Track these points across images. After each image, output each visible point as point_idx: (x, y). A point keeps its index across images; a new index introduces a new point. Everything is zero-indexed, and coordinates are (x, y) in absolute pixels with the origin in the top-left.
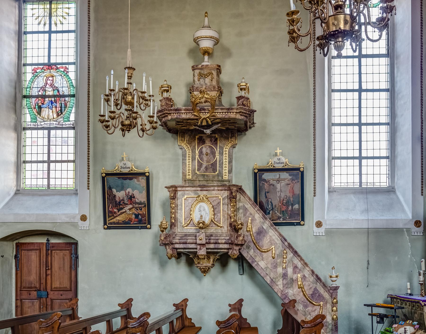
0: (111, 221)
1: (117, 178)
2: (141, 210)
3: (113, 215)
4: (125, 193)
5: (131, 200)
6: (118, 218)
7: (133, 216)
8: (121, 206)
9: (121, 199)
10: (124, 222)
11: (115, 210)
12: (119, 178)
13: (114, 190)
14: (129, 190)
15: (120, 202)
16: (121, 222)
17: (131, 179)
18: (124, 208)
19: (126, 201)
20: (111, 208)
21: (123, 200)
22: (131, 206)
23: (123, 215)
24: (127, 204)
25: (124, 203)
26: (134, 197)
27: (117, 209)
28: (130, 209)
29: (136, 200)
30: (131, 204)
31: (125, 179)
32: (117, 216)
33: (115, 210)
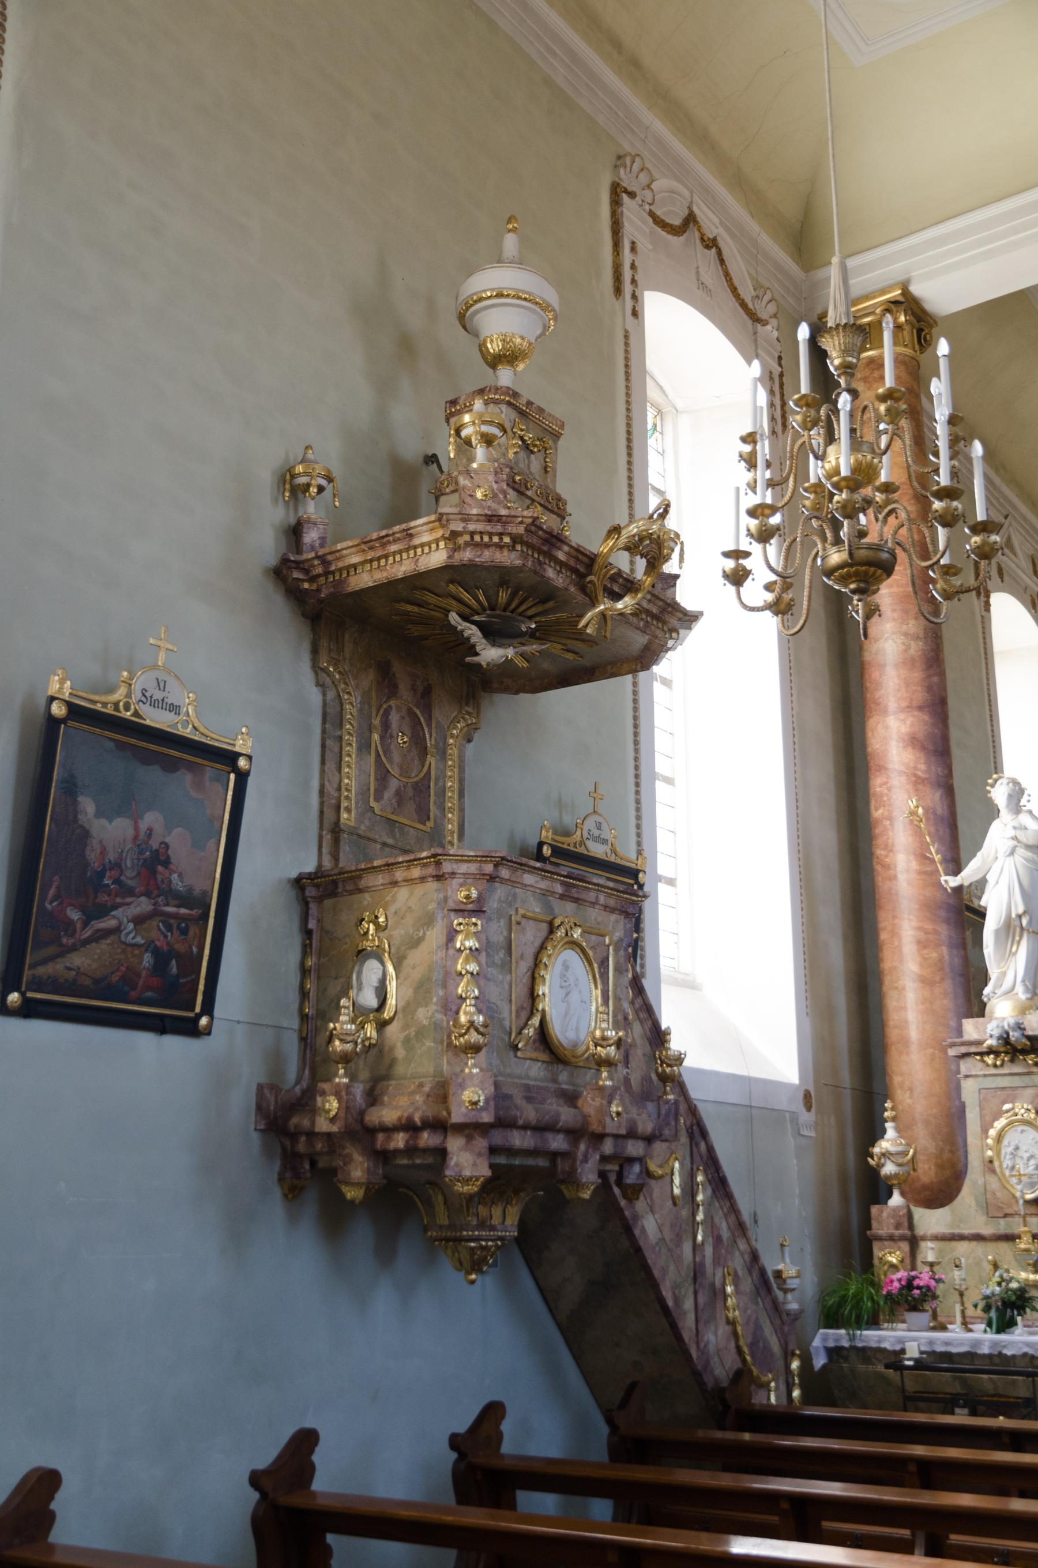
0: (42, 971)
1: (112, 745)
2: (184, 932)
4: (131, 832)
5: (153, 872)
6: (78, 960)
7: (147, 959)
8: (103, 898)
9: (112, 856)
10: (104, 988)
11: (74, 915)
12: (120, 746)
13: (88, 806)
14: (151, 819)
15: (101, 875)
16: (87, 982)
17: (171, 766)
18: (115, 907)
19: (129, 873)
20: (56, 898)
21: (117, 865)
22: (143, 905)
23: (104, 945)
24: (131, 892)
25: (117, 881)
26: (167, 863)
27: (82, 909)
28: (139, 921)
29: (175, 877)
30: (148, 894)
31: (147, 759)
32: (73, 949)
33: (74, 915)
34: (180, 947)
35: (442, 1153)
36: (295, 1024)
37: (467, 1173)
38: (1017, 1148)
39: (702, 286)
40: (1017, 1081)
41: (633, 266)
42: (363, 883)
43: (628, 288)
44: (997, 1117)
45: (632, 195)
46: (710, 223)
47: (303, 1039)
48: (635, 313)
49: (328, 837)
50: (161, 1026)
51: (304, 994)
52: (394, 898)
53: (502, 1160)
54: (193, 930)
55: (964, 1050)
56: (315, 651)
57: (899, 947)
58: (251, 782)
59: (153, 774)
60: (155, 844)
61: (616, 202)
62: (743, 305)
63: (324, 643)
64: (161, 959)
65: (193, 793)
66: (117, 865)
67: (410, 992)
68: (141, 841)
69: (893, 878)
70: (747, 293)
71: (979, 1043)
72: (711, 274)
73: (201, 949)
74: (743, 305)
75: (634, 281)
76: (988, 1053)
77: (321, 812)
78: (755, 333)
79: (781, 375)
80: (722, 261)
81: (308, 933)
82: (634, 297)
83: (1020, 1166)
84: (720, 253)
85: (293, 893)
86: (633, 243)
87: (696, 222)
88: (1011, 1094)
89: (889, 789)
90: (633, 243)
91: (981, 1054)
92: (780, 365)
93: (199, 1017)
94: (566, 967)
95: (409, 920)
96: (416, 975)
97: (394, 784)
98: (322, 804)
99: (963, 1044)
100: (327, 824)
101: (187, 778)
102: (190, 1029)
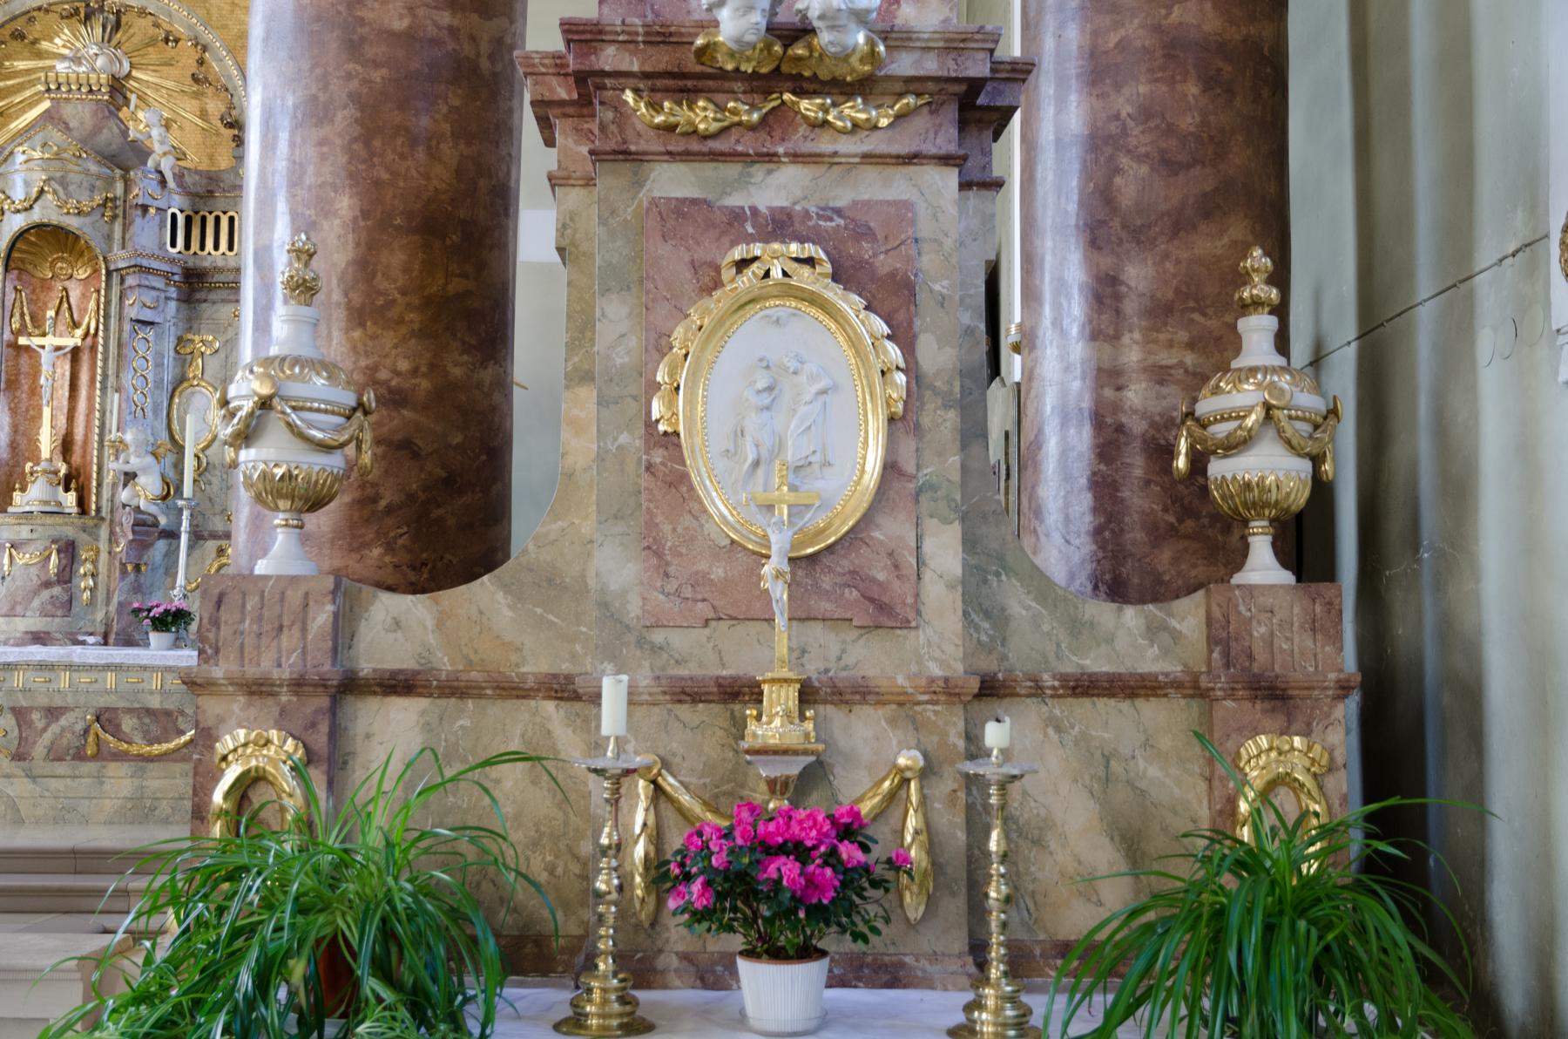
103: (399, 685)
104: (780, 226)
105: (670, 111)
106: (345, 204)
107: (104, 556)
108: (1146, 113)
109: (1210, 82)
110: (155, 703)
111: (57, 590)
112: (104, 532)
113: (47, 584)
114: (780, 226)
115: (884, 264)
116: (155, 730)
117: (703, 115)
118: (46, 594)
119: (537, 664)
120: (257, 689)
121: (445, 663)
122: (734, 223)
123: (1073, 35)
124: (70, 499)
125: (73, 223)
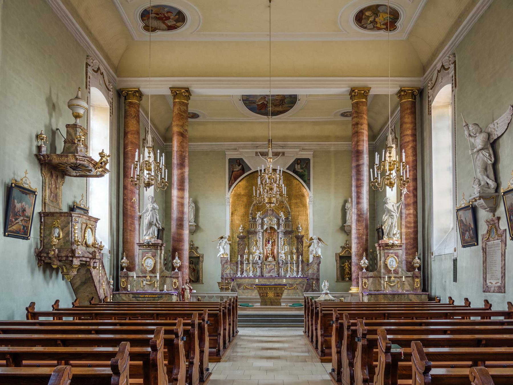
0: (9, 229)
1: (19, 191)
2: (27, 222)
3: (11, 224)
4: (21, 206)
5: (23, 212)
6: (14, 227)
7: (22, 227)
8: (17, 217)
9: (18, 210)
10: (17, 232)
11: (14, 220)
12: (20, 191)
13: (16, 201)
14: (24, 203)
15: (17, 213)
16: (15, 231)
17: (26, 194)
18: (19, 218)
19: (21, 213)
20: (12, 217)
21: (19, 211)
22: (22, 218)
23: (17, 225)
24: (20, 216)
25: (19, 214)
26: (25, 211)
27: (15, 219)
28: (21, 221)
29: (26, 213)
30: (23, 216)
31: (23, 193)
32: (13, 225)
33: (14, 220)
34: (26, 225)
35: (72, 261)
36: (39, 238)
37: (76, 264)
38: (148, 262)
39: (100, 84)
40: (149, 251)
41: (89, 82)
42: (54, 215)
43: (88, 87)
44: (145, 256)
45: (90, 66)
46: (102, 69)
47: (41, 241)
48: (89, 93)
49: (43, 204)
50: (24, 238)
51: (41, 233)
52: (61, 219)
53: (82, 262)
54: (28, 222)
55: (140, 245)
56: (41, 170)
57: (128, 224)
58: (37, 196)
59: (24, 195)
60: (24, 208)
61: (87, 67)
62: (107, 87)
63: (43, 169)
64: (24, 227)
65: (29, 199)
66: (19, 211)
67: (65, 235)
68: (22, 207)
69: (127, 211)
70: (107, 84)
71: (143, 244)
72: (102, 82)
73: (29, 225)
74: (107, 87)
75: (89, 85)
76: (144, 246)
77: (42, 200)
78: (108, 93)
79: (112, 102)
80: (104, 78)
81: (41, 222)
82: (89, 89)
83: (148, 265)
84: (103, 76)
85: (39, 215)
86: (89, 76)
87: (100, 69)
88: (147, 253)
89: (128, 193)
90: (89, 76)
91: (143, 246)
92: (112, 100)
93: (28, 237)
94: (89, 231)
95: (64, 223)
96: (66, 232)
97: (53, 194)
98: (42, 198)
99: (140, 244)
100: (43, 202)
101: (28, 196)
102: (27, 239)
103: (371, 277)
104: (392, 253)
105: (386, 247)
106: (361, 249)
107: (278, 266)
108: (409, 242)
109: (413, 240)
110: (291, 283)
111: (273, 270)
112: (277, 263)
113: (272, 270)
114: (392, 253)
115: (397, 255)
116: (290, 286)
117: (388, 247)
118: (272, 271)
119: (378, 276)
120: (365, 277)
121: (374, 276)
122: (389, 253)
123: (404, 237)
124: (274, 259)
125: (273, 226)
